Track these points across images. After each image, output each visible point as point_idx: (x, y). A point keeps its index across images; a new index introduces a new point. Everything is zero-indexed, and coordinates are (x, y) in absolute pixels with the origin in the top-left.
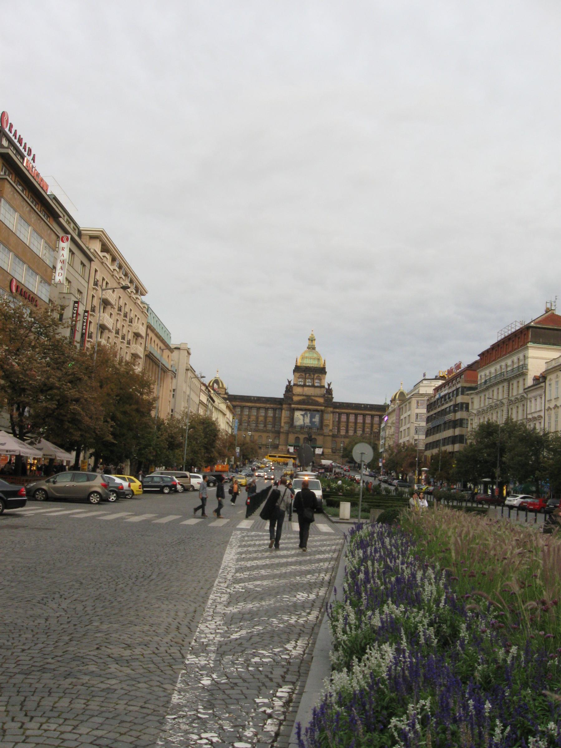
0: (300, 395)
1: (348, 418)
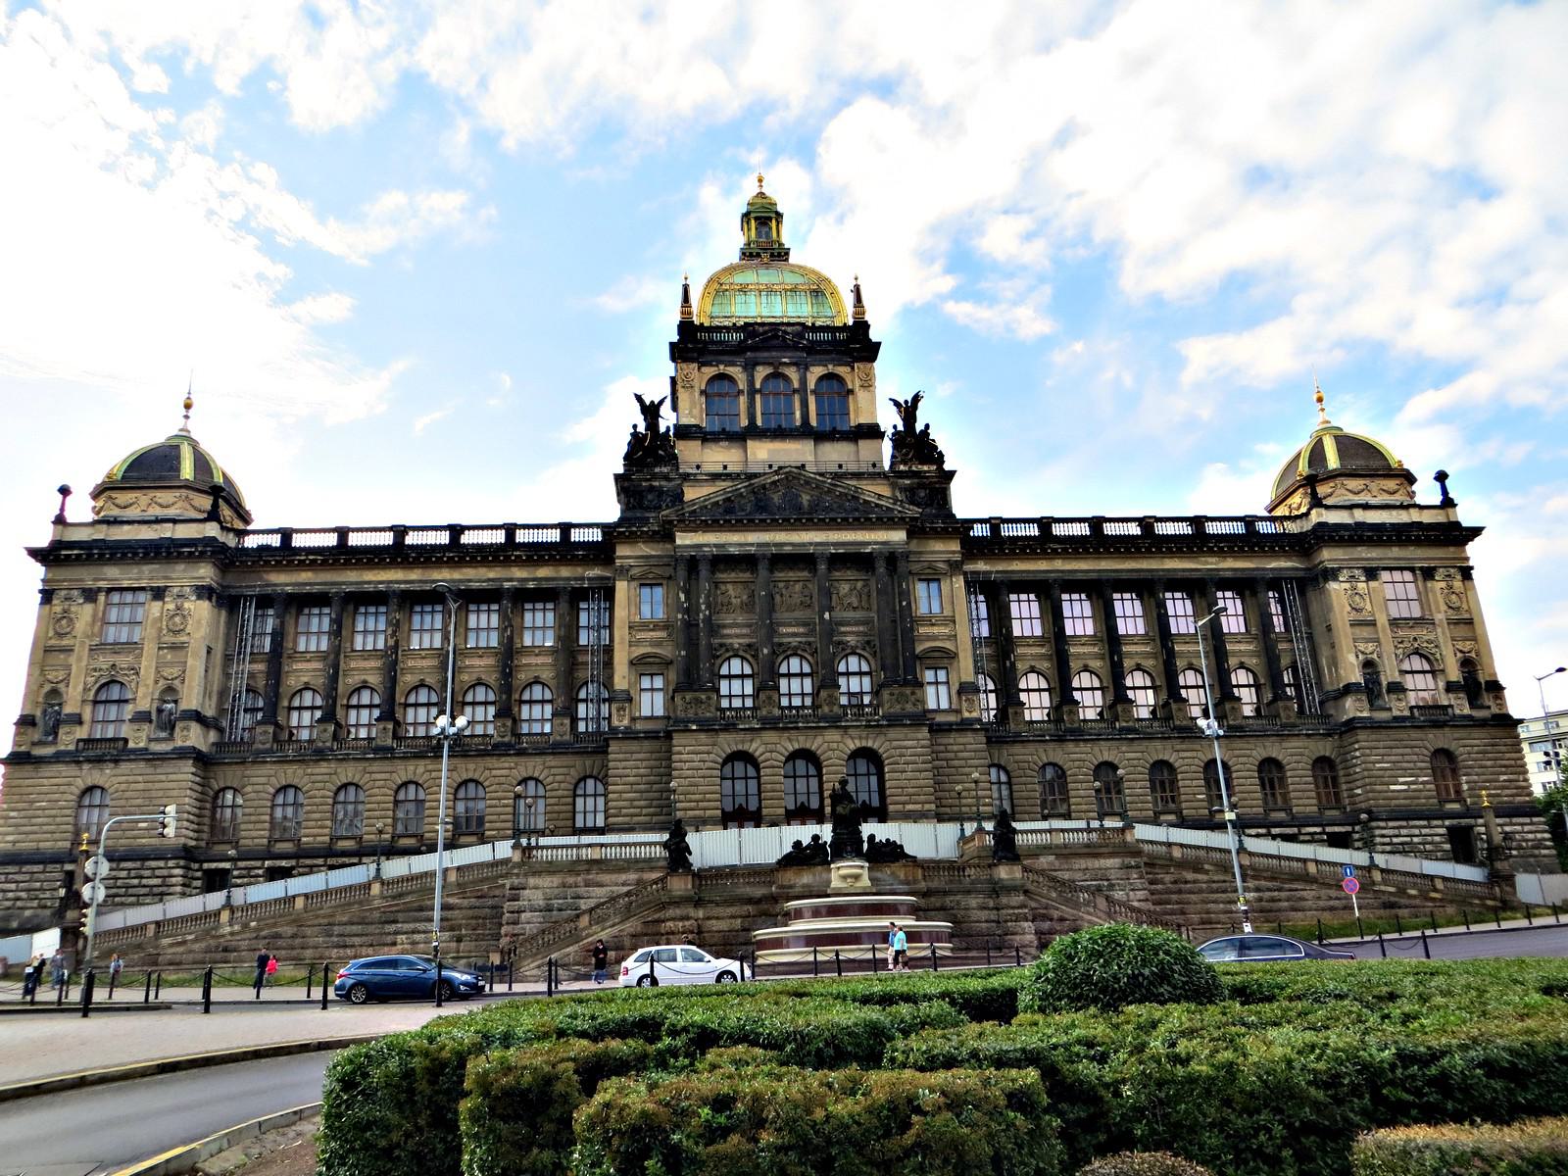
0: (729, 476)
1: (1054, 616)
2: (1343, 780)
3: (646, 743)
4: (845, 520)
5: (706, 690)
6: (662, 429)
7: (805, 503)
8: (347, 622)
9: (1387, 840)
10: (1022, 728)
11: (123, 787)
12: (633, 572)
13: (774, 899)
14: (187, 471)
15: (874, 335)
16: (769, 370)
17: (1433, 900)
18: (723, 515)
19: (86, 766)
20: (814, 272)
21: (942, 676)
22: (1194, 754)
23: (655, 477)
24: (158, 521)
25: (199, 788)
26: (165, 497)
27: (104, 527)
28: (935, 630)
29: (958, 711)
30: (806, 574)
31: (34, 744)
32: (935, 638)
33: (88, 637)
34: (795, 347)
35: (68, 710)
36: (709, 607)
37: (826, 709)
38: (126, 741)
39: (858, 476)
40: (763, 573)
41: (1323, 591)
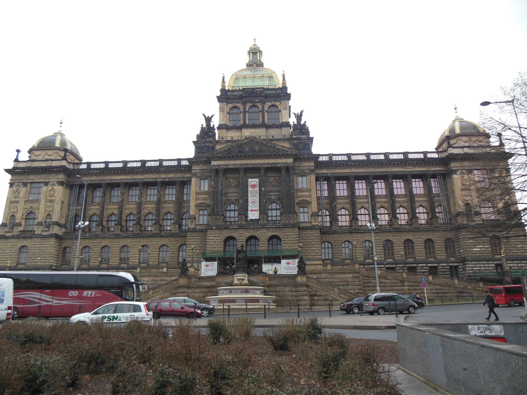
1: (351, 189)
2: (456, 246)
3: (199, 233)
4: (270, 155)
5: (219, 215)
6: (212, 126)
7: (257, 150)
8: (108, 193)
9: (471, 268)
10: (337, 228)
11: (33, 246)
12: (198, 174)
13: (214, 287)
14: (57, 144)
15: (289, 91)
16: (251, 104)
17: (479, 290)
18: (228, 155)
19: (22, 239)
20: (270, 70)
21: (306, 210)
22: (400, 237)
23: (206, 142)
24: (47, 160)
25: (58, 247)
26: (50, 152)
27: (30, 162)
28: (304, 194)
29: (311, 222)
30: (258, 174)
31: (6, 232)
32: (303, 196)
33: (24, 198)
34: (260, 96)
35: (17, 221)
36: (222, 186)
37: (261, 222)
38: (34, 231)
39: (278, 140)
40: (242, 175)
41: (451, 178)
